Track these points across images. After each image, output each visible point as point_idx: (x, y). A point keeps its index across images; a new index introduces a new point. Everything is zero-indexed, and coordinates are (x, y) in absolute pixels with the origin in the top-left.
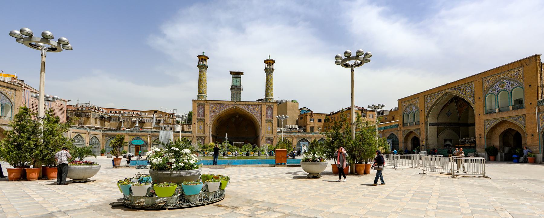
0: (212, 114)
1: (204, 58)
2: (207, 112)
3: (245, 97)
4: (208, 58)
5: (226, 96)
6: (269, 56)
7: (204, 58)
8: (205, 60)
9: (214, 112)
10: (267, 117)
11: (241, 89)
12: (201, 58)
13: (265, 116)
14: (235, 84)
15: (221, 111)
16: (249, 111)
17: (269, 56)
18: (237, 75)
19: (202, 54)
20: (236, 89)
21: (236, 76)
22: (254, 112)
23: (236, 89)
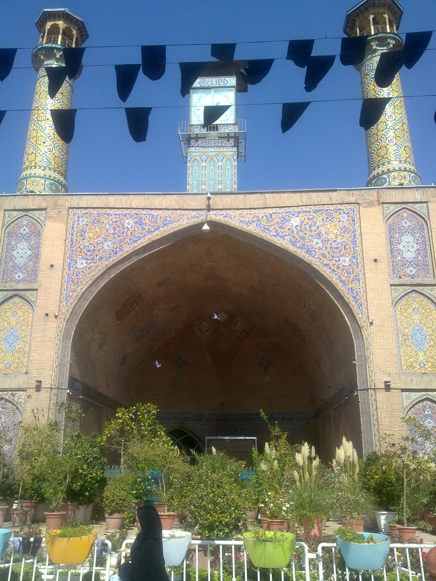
0: (81, 264)
9: (90, 254)
10: (396, 267)
13: (384, 266)
22: (317, 243)
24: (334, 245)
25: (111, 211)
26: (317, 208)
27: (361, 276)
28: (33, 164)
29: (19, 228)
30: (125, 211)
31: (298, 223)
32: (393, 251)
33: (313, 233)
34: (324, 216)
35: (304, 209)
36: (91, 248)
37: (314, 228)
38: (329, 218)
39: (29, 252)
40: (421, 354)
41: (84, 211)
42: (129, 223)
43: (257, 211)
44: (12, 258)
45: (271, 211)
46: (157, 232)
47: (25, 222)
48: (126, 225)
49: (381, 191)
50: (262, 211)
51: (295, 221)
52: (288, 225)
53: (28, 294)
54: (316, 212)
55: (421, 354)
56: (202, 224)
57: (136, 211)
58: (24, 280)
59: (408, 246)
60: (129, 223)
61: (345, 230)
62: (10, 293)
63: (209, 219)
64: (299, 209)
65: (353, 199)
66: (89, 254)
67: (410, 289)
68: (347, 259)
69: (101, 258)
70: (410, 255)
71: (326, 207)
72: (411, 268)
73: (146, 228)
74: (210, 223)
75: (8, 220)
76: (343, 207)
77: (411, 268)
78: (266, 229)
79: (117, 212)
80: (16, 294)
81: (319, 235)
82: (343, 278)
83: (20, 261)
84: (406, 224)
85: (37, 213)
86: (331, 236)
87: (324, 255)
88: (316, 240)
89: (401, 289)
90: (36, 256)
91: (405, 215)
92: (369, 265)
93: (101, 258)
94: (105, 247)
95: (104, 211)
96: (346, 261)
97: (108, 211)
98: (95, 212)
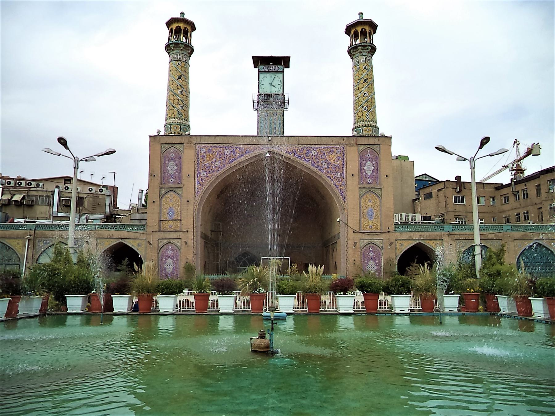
0: (203, 174)
1: (182, 26)
2: (188, 167)
3: (295, 124)
4: (194, 29)
5: (243, 122)
6: (361, 14)
7: (182, 26)
8: (186, 33)
9: (209, 170)
11: (283, 103)
12: (174, 26)
13: (356, 178)
14: (267, 89)
15: (227, 166)
16: (309, 165)
17: (361, 14)
18: (272, 64)
19: (178, 16)
20: (271, 104)
21: (268, 67)
22: (325, 165)
23: (271, 104)
24: (333, 166)
25: (218, 145)
26: (325, 146)
27: (345, 183)
28: (173, 116)
29: (170, 154)
30: (225, 145)
31: (316, 154)
32: (361, 170)
33: (323, 160)
34: (329, 150)
35: (319, 146)
36: (208, 166)
37: (323, 157)
38: (332, 151)
39: (176, 167)
40: (370, 222)
41: (204, 145)
42: (228, 152)
43: (294, 146)
44: (167, 170)
45: (302, 147)
46: (242, 157)
47: (172, 151)
48: (226, 153)
49: (358, 138)
50: (297, 146)
51: (314, 153)
52: (310, 155)
53: (177, 190)
54: (325, 148)
55: (370, 222)
56: (266, 153)
57: (231, 145)
58: (174, 183)
59: (369, 168)
60: (228, 152)
61: (338, 158)
62: (168, 190)
63: (269, 150)
64: (316, 146)
65: (343, 142)
66: (207, 169)
67: (368, 190)
68: (339, 174)
69: (214, 171)
70: (369, 173)
71: (330, 146)
72: (369, 179)
73: (237, 155)
74: (270, 152)
75: (163, 149)
76: (338, 146)
77: (369, 179)
78: (299, 157)
79: (221, 146)
80: (171, 189)
81: (326, 161)
82: (337, 184)
83: (171, 172)
84: (368, 156)
85: (178, 146)
86: (332, 161)
87: (328, 172)
88: (324, 164)
89: (364, 190)
90: (180, 169)
91: (369, 151)
92: (349, 177)
93: (214, 171)
94: (216, 165)
95: (214, 145)
96: (338, 175)
97: (216, 145)
98: (209, 145)
